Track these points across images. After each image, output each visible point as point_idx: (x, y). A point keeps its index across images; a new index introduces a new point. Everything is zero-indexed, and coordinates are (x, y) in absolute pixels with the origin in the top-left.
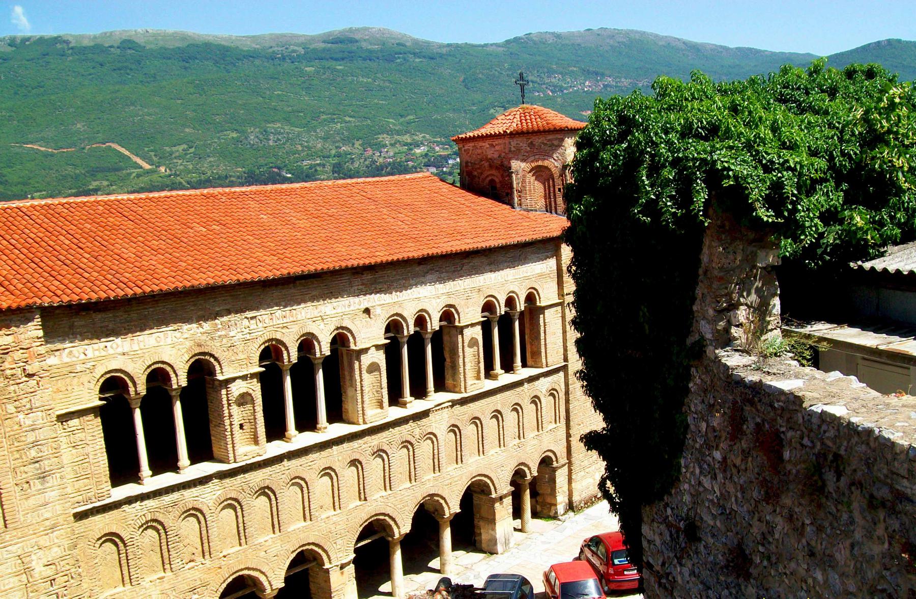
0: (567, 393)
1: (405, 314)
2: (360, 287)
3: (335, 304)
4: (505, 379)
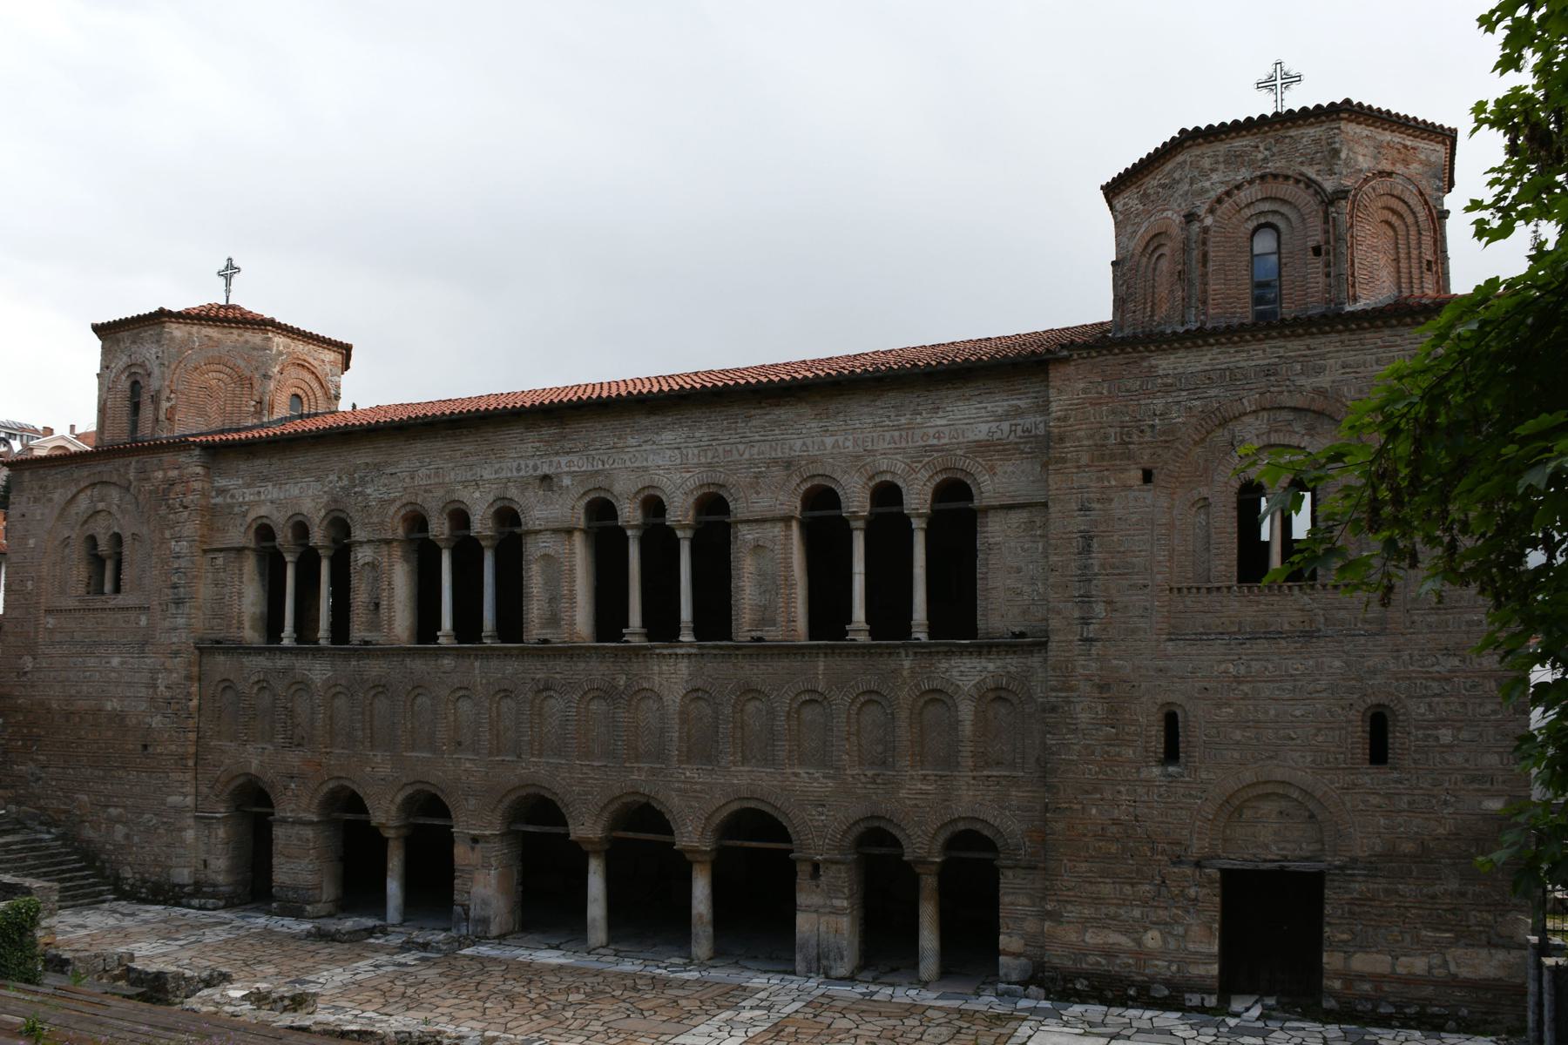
1: (618, 488)
2: (538, 444)
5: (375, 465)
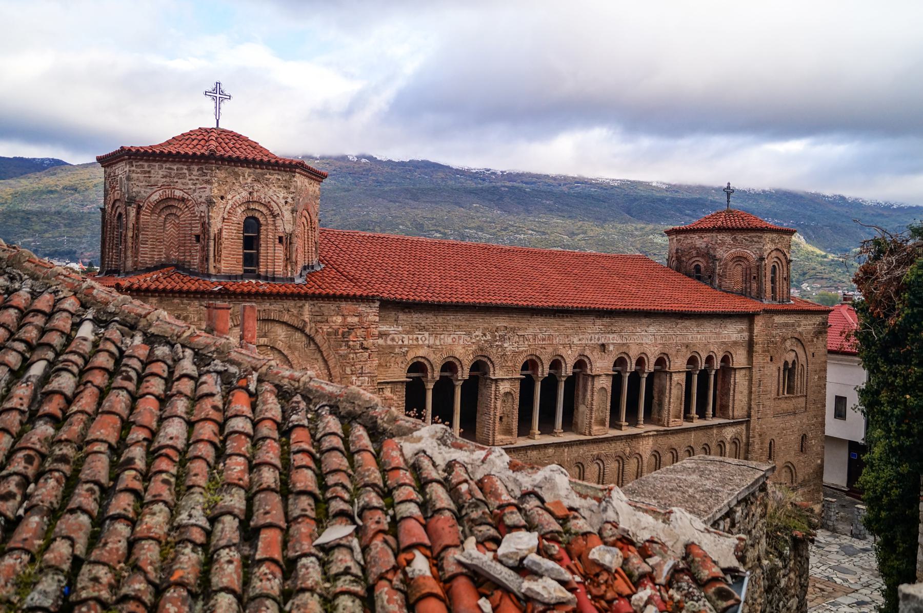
0: (748, 444)
2: (601, 327)
3: (581, 337)
4: (697, 423)
5: (511, 328)
